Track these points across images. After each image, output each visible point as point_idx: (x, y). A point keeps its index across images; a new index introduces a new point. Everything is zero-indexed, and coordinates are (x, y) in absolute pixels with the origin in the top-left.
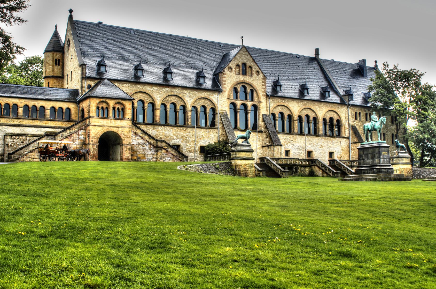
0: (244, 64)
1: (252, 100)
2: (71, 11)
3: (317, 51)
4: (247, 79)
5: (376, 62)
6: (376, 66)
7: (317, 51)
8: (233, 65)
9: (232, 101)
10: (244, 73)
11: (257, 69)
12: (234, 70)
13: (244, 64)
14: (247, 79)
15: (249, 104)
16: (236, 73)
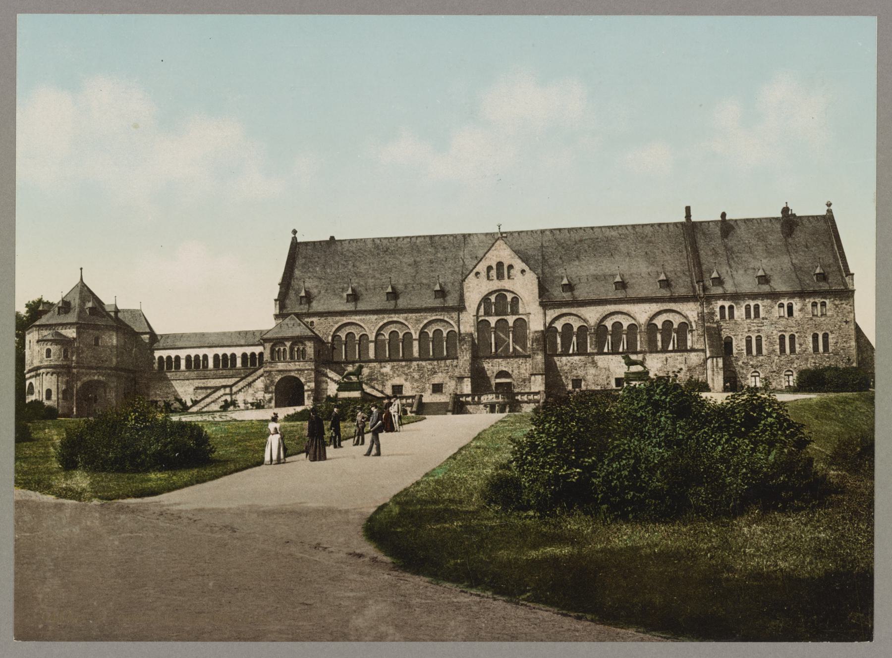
0: (500, 265)
1: (515, 312)
2: (295, 232)
3: (688, 209)
4: (506, 284)
5: (829, 205)
6: (829, 211)
7: (688, 209)
8: (482, 267)
9: (480, 319)
10: (500, 276)
11: (524, 266)
12: (483, 274)
13: (500, 265)
14: (506, 284)
15: (511, 320)
16: (488, 278)
